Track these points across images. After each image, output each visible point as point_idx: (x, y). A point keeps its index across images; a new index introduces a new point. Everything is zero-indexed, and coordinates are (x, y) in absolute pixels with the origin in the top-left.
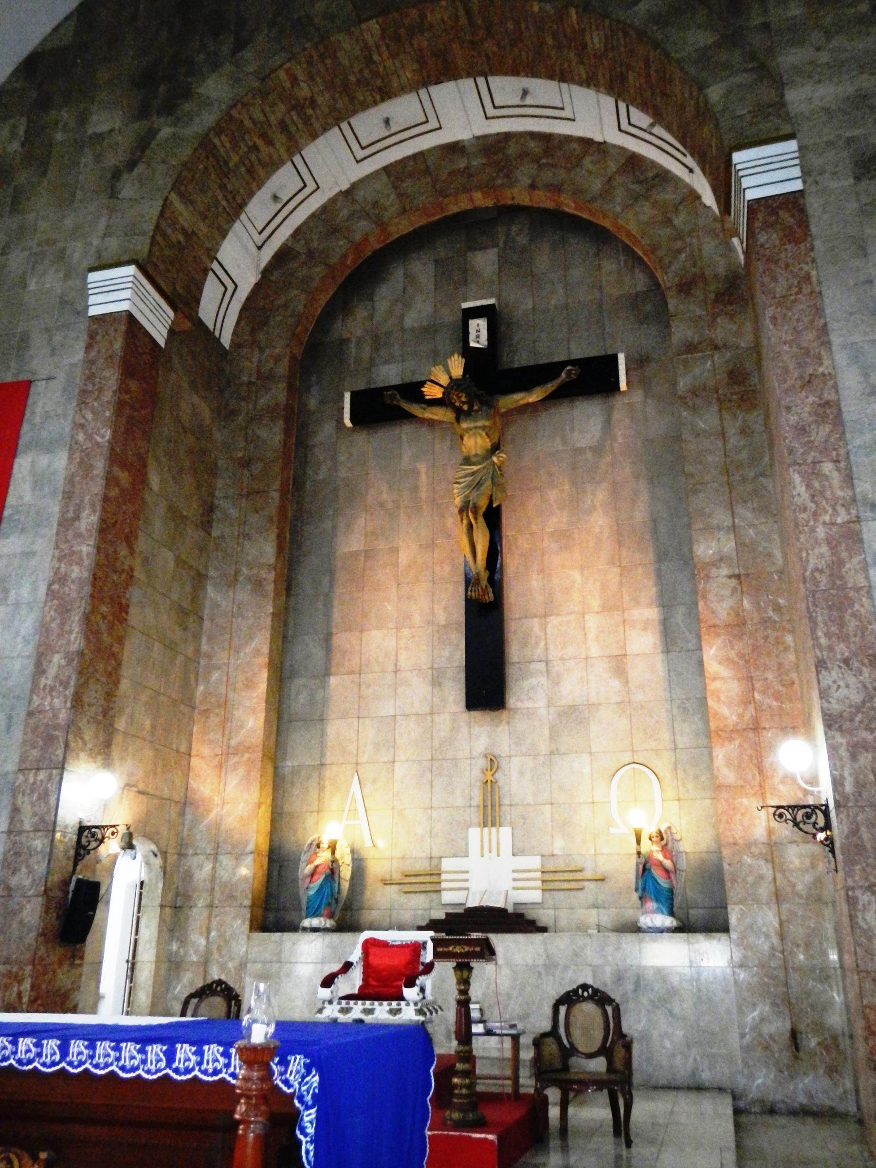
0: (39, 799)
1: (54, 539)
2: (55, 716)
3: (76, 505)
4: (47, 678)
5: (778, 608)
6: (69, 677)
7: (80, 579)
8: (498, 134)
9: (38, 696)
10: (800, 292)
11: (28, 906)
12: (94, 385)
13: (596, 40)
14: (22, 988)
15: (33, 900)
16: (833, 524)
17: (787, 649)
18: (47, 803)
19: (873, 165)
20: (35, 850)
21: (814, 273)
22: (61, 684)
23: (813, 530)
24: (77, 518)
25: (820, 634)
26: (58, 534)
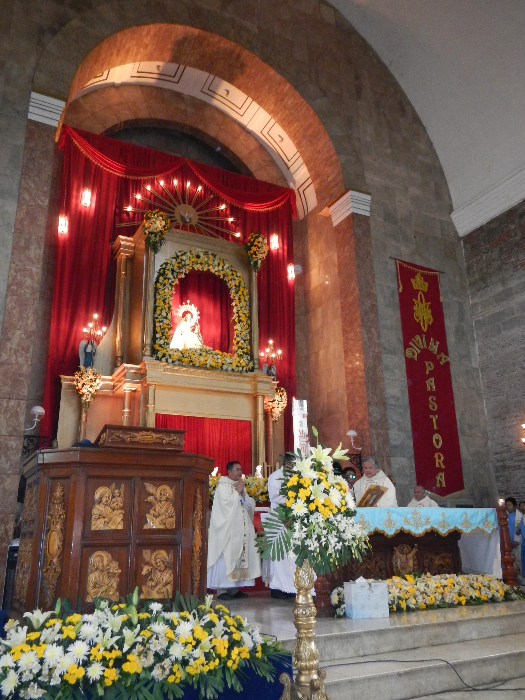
0: (11, 416)
1: (10, 255)
2: (20, 367)
3: (25, 239)
4: (12, 344)
5: (304, 373)
6: (28, 347)
7: (32, 287)
8: (201, 100)
9: (6, 353)
10: (367, 258)
11: (8, 479)
12: (34, 166)
13: (290, 102)
14: (7, 527)
15: (12, 476)
16: (374, 352)
17: (306, 390)
18: (18, 420)
19: (389, 217)
20: (11, 447)
21: (371, 252)
22: (23, 349)
23: (369, 353)
24: (27, 247)
25: (369, 392)
26: (12, 253)
